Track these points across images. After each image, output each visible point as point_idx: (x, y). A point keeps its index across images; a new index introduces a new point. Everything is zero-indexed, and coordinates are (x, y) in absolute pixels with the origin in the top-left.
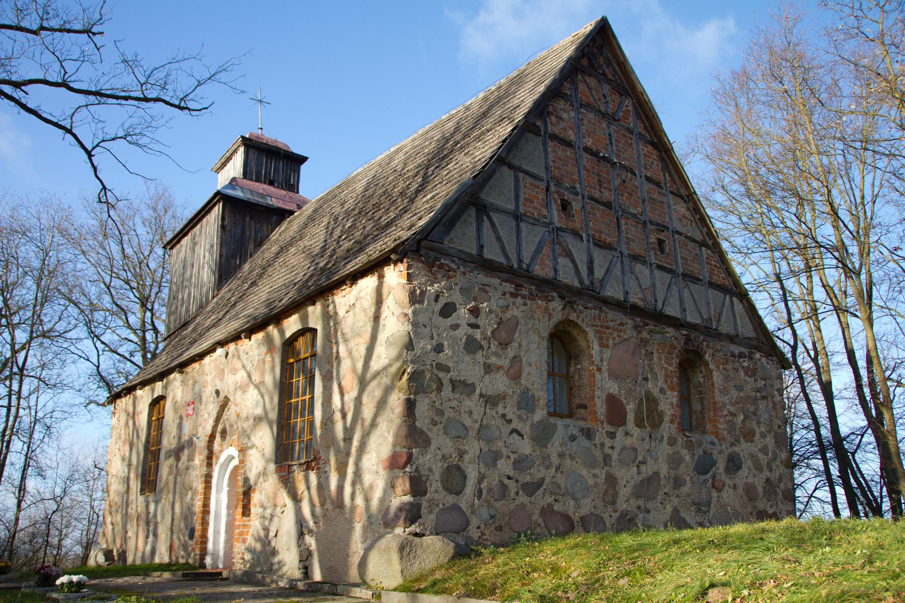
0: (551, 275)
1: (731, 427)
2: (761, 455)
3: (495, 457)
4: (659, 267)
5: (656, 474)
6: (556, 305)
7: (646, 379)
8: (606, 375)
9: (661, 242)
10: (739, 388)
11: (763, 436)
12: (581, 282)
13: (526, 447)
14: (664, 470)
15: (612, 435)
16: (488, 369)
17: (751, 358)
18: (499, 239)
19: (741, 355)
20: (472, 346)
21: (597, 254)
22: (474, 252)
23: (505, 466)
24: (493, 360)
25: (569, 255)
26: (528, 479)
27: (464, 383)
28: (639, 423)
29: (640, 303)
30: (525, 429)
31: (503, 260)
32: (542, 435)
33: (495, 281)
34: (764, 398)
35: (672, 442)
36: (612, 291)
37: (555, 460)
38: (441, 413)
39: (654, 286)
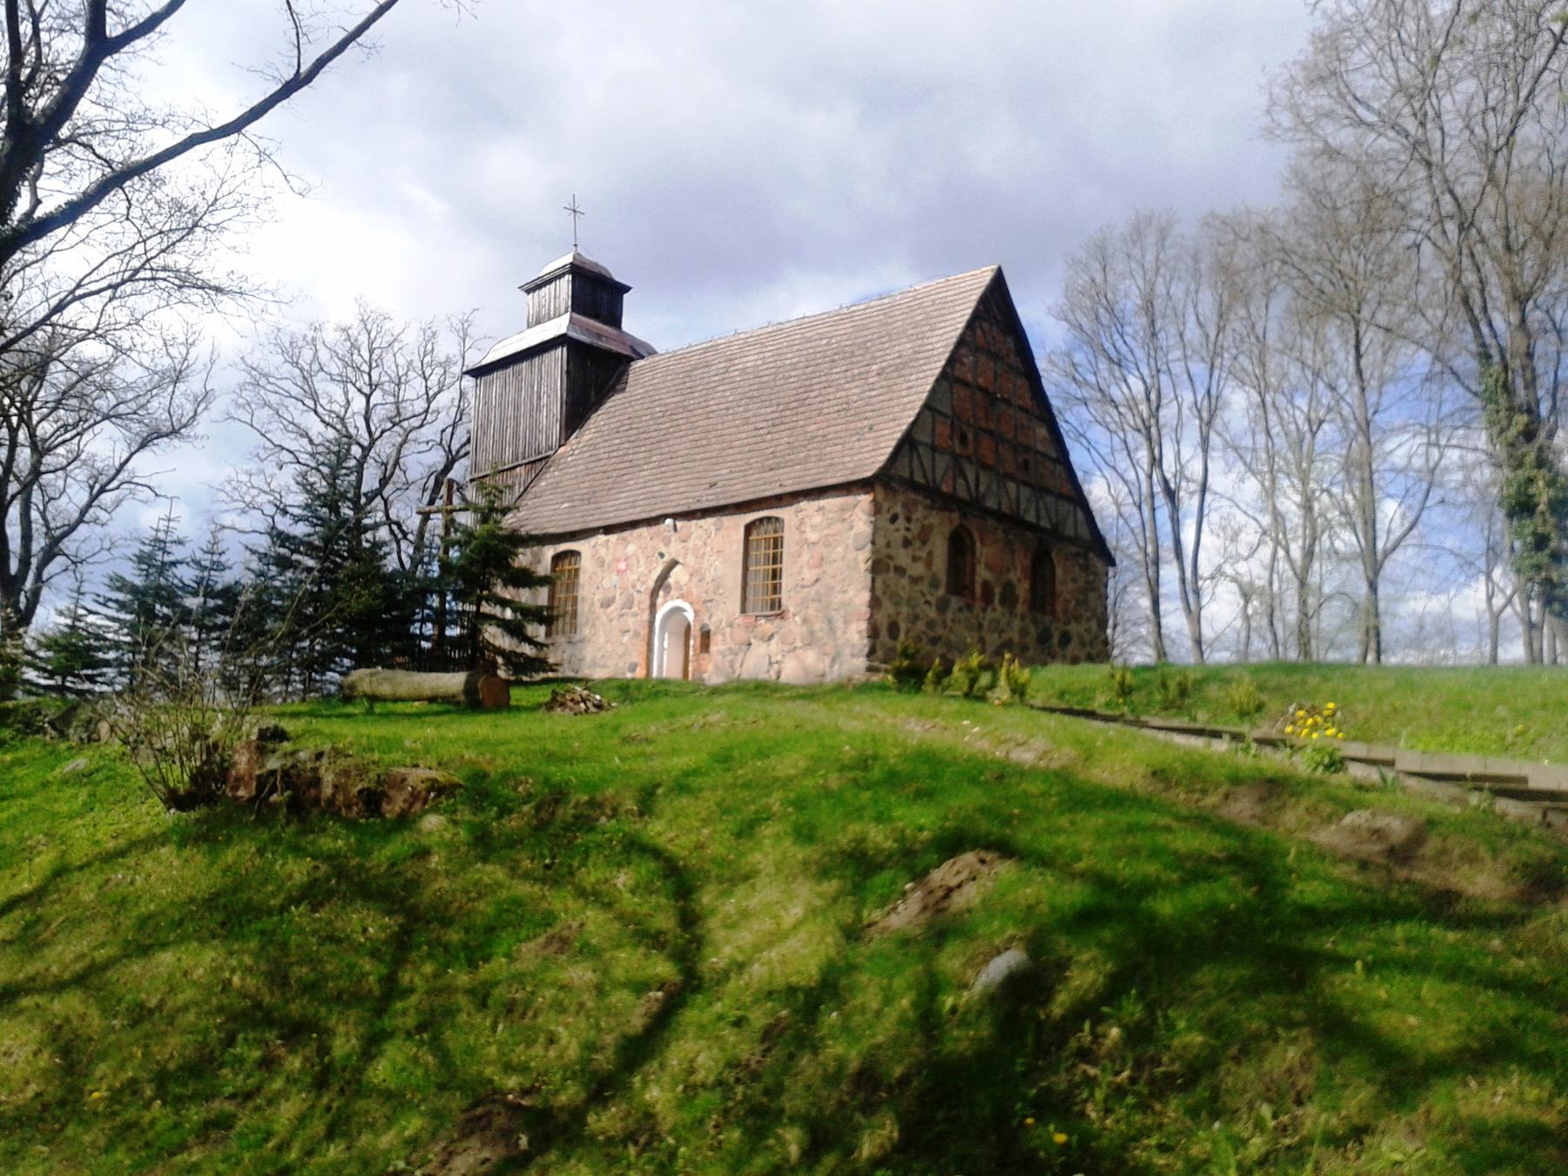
1: (1065, 611)
3: (917, 617)
6: (956, 516)
10: (1075, 580)
11: (1088, 620)
14: (1016, 637)
15: (984, 610)
16: (915, 559)
19: (1077, 555)
20: (907, 543)
22: (907, 475)
23: (921, 626)
28: (1003, 601)
32: (942, 606)
35: (1023, 618)
36: (991, 503)
37: (949, 623)
39: (1018, 498)
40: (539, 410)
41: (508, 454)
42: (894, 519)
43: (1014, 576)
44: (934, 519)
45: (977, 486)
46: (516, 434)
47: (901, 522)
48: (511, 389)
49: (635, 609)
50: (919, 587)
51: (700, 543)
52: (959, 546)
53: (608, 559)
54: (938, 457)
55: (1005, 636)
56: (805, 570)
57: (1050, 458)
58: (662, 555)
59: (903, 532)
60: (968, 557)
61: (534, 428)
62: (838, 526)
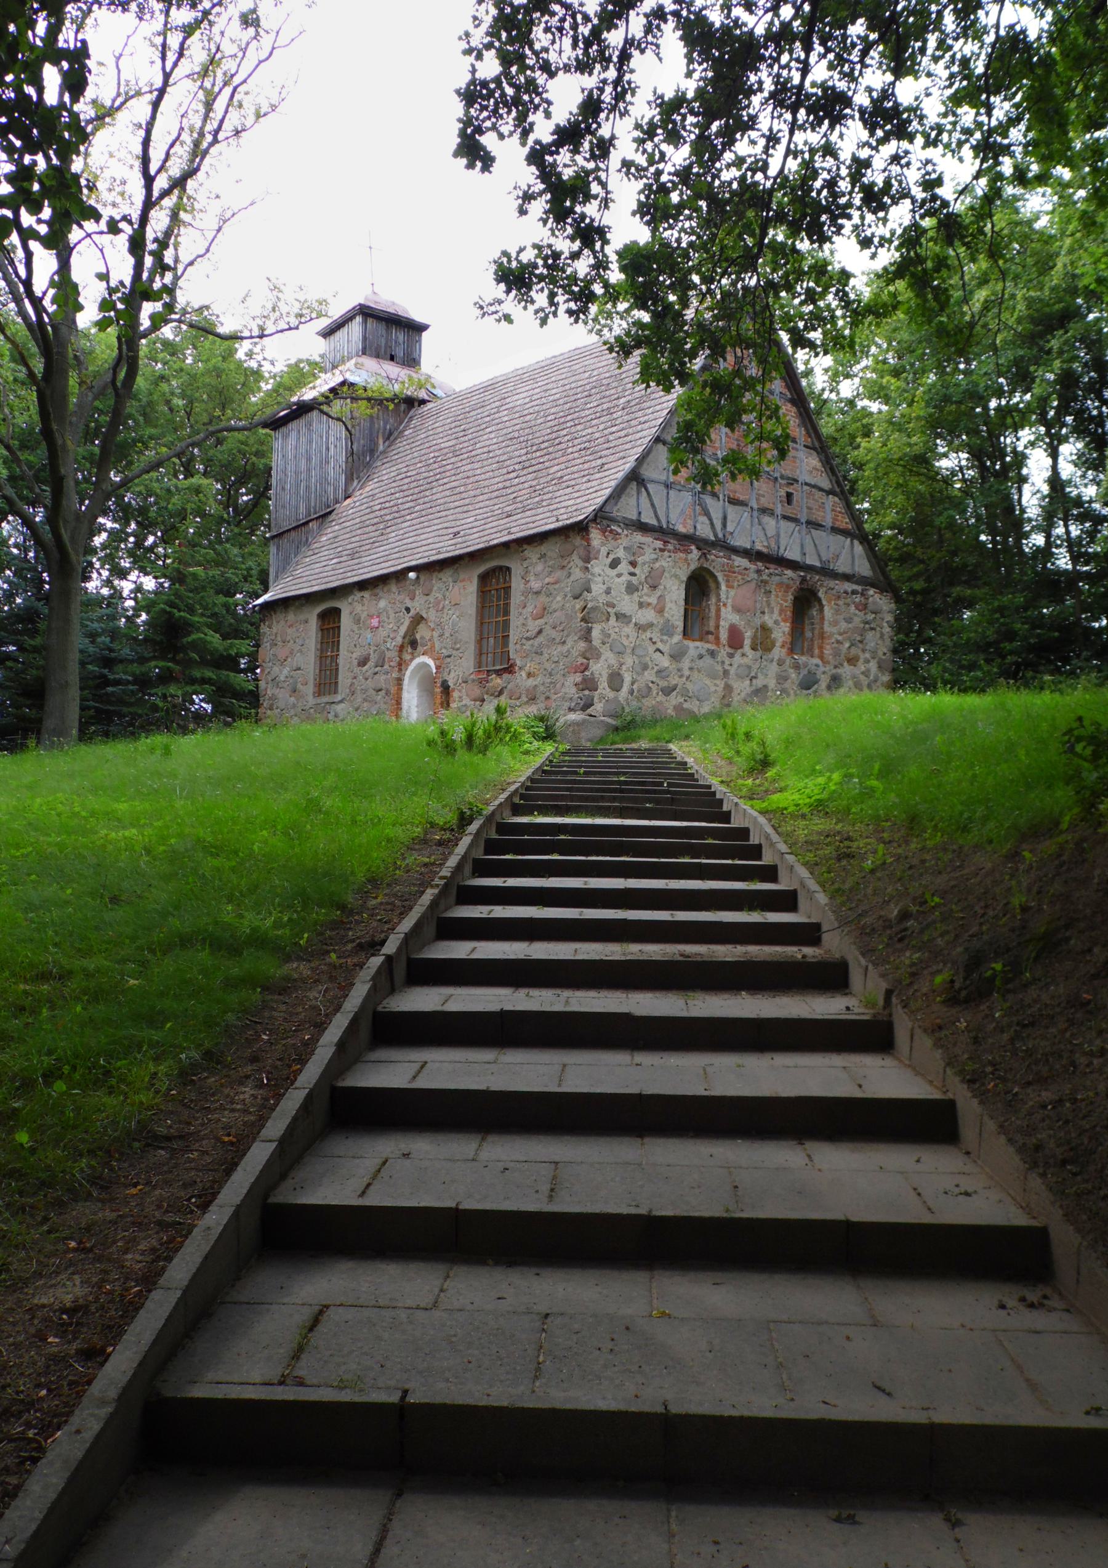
0: (692, 531)
1: (836, 653)
2: (862, 677)
3: (645, 667)
4: (785, 517)
5: (765, 687)
6: (695, 553)
7: (763, 613)
8: (730, 608)
9: (789, 496)
10: (849, 620)
11: (867, 661)
12: (716, 535)
13: (665, 662)
14: (772, 683)
15: (731, 656)
16: (641, 605)
17: (862, 594)
18: (653, 505)
19: (854, 592)
20: (631, 589)
21: (732, 511)
22: (634, 518)
23: (649, 675)
24: (645, 599)
25: (707, 514)
26: (666, 684)
27: (624, 616)
29: (765, 550)
30: (665, 648)
31: (654, 522)
32: (677, 656)
33: (648, 539)
34: (872, 629)
35: (781, 663)
37: (687, 673)
38: (609, 636)
39: (778, 535)
40: (328, 462)
41: (302, 510)
42: (614, 564)
43: (768, 620)
44: (665, 562)
45: (724, 525)
46: (308, 487)
47: (624, 567)
48: (303, 439)
49: (386, 667)
50: (648, 634)
51: (440, 596)
52: (699, 586)
53: (364, 616)
54: (672, 492)
55: (759, 683)
56: (530, 622)
57: (821, 489)
58: (408, 610)
59: (626, 578)
60: (713, 600)
61: (324, 480)
62: (559, 574)
